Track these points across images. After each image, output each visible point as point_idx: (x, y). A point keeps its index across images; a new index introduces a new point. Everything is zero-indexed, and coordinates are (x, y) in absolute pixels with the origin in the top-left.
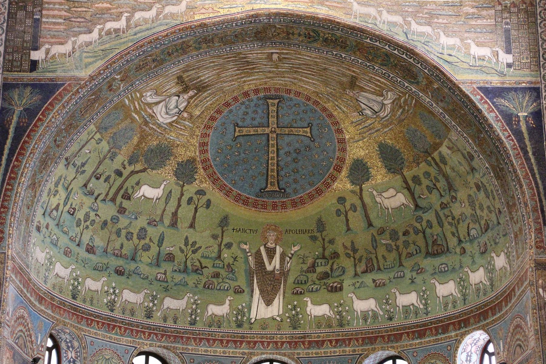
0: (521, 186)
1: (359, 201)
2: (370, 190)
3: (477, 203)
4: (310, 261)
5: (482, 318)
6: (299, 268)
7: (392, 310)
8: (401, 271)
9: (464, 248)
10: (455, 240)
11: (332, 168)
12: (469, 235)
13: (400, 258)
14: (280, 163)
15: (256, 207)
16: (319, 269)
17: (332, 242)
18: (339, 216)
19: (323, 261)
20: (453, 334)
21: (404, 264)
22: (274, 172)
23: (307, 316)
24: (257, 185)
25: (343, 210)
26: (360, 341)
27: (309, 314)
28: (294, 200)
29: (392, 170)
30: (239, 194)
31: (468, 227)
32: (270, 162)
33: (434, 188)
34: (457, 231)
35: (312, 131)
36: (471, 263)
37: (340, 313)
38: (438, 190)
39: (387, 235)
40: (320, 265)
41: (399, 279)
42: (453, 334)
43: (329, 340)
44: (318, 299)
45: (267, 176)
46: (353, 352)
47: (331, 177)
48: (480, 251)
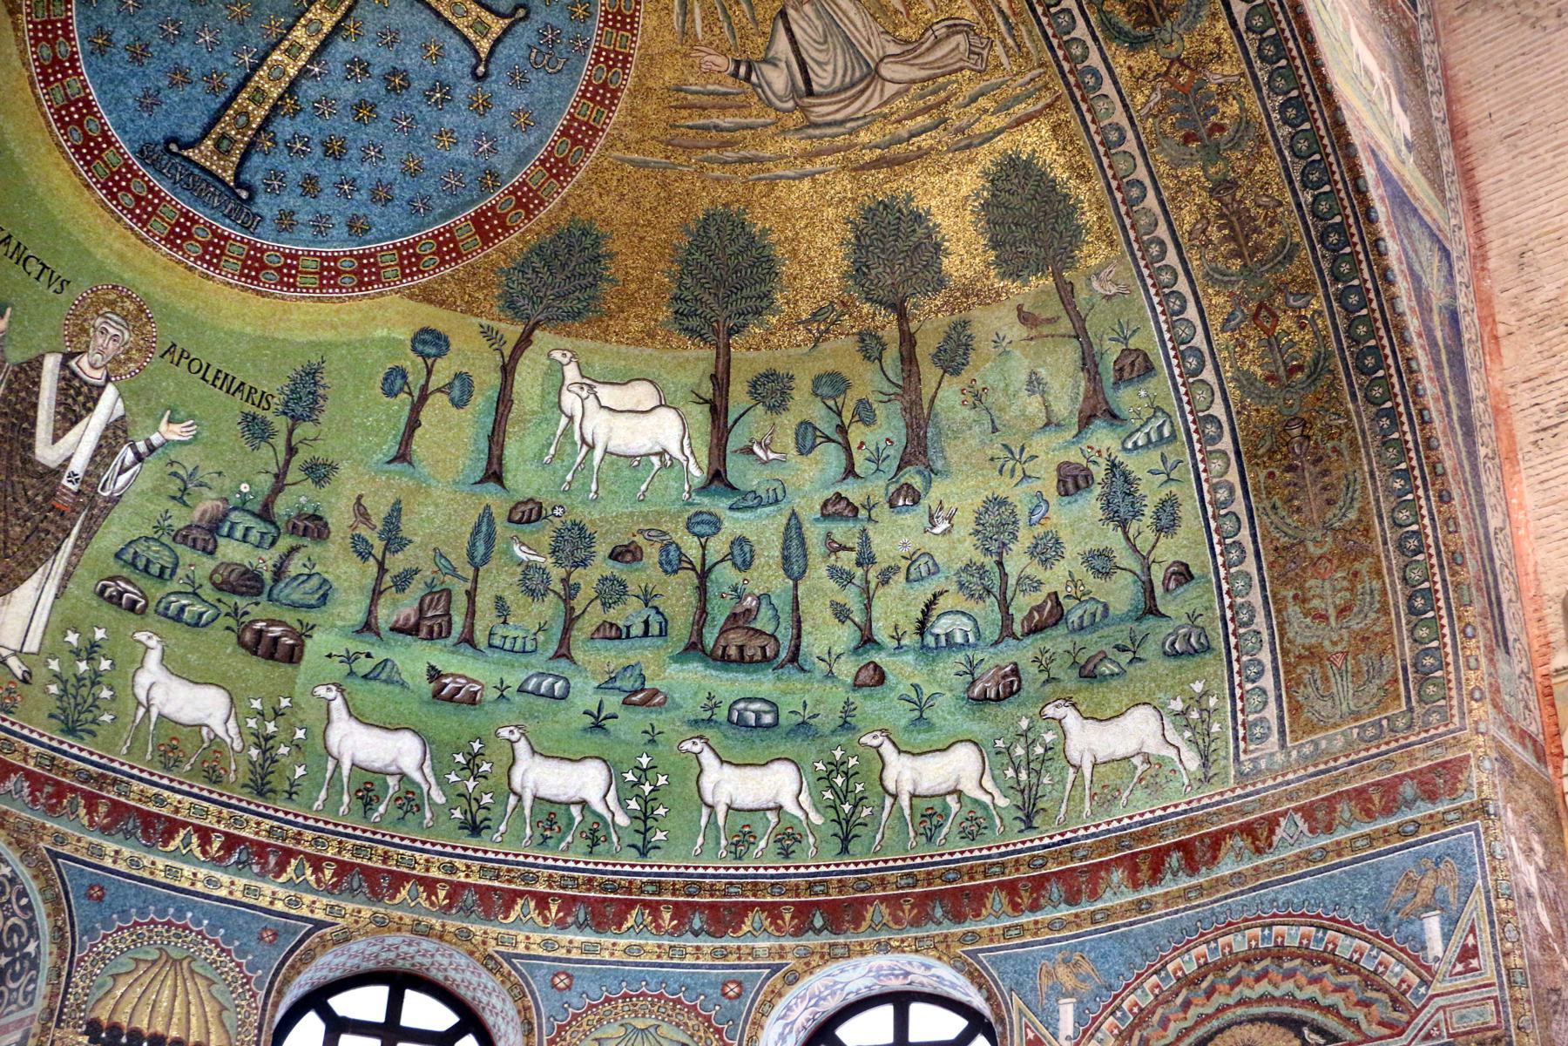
0: (1444, 498)
1: (495, 379)
2: (557, 355)
3: (1025, 538)
4: (206, 504)
5: (939, 913)
6: (156, 508)
7: (486, 799)
8: (558, 678)
9: (876, 667)
10: (845, 636)
11: (471, 212)
12: (922, 627)
13: (567, 630)
14: (306, 84)
15: (114, 196)
16: (232, 551)
17: (319, 472)
18: (390, 393)
19: (258, 527)
20: (767, 944)
21: (578, 655)
22: (259, 104)
23: (131, 704)
24: (168, 114)
25: (416, 380)
26: (328, 873)
27: (142, 697)
28: (263, 251)
29: (694, 323)
30: (88, 104)
31: (929, 606)
32: (276, 56)
33: (829, 440)
34: (868, 608)
35: (508, 41)
36: (903, 722)
37: (265, 742)
38: (847, 449)
39: (545, 534)
40: (238, 534)
41: (542, 701)
42: (763, 944)
43: (198, 829)
44: (192, 658)
45: (226, 105)
46: (289, 904)
47: (446, 242)
48: (968, 690)
